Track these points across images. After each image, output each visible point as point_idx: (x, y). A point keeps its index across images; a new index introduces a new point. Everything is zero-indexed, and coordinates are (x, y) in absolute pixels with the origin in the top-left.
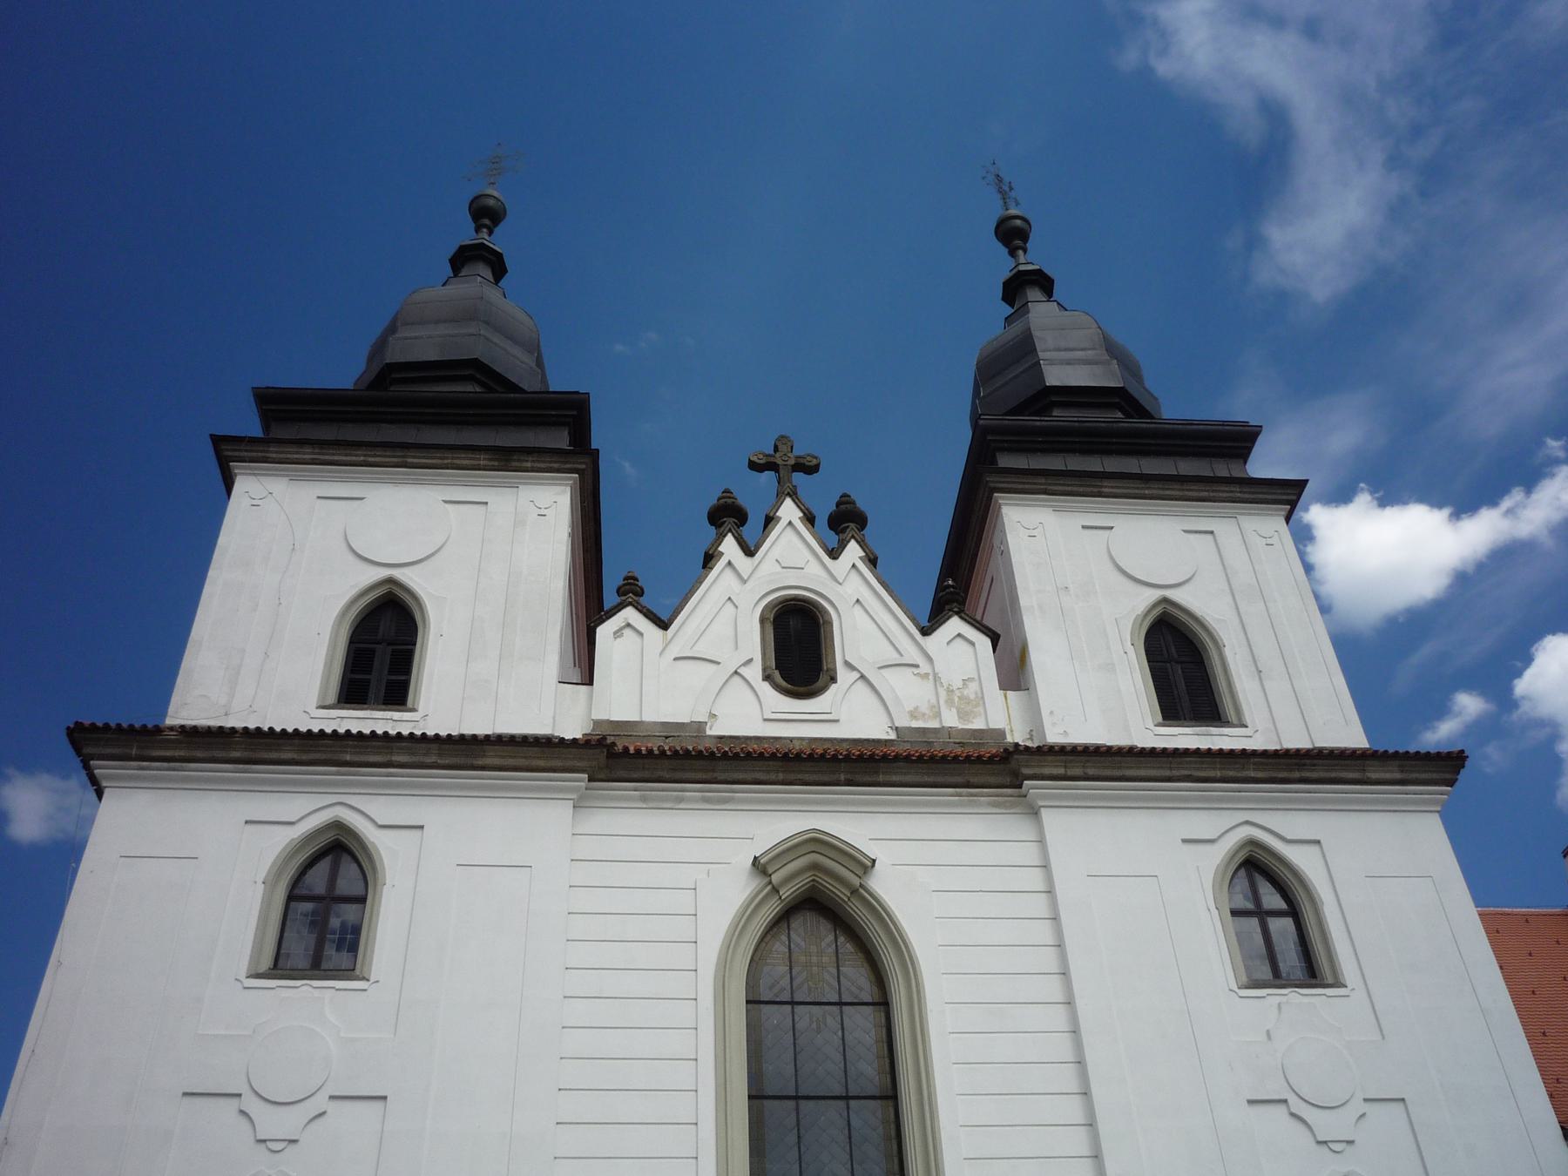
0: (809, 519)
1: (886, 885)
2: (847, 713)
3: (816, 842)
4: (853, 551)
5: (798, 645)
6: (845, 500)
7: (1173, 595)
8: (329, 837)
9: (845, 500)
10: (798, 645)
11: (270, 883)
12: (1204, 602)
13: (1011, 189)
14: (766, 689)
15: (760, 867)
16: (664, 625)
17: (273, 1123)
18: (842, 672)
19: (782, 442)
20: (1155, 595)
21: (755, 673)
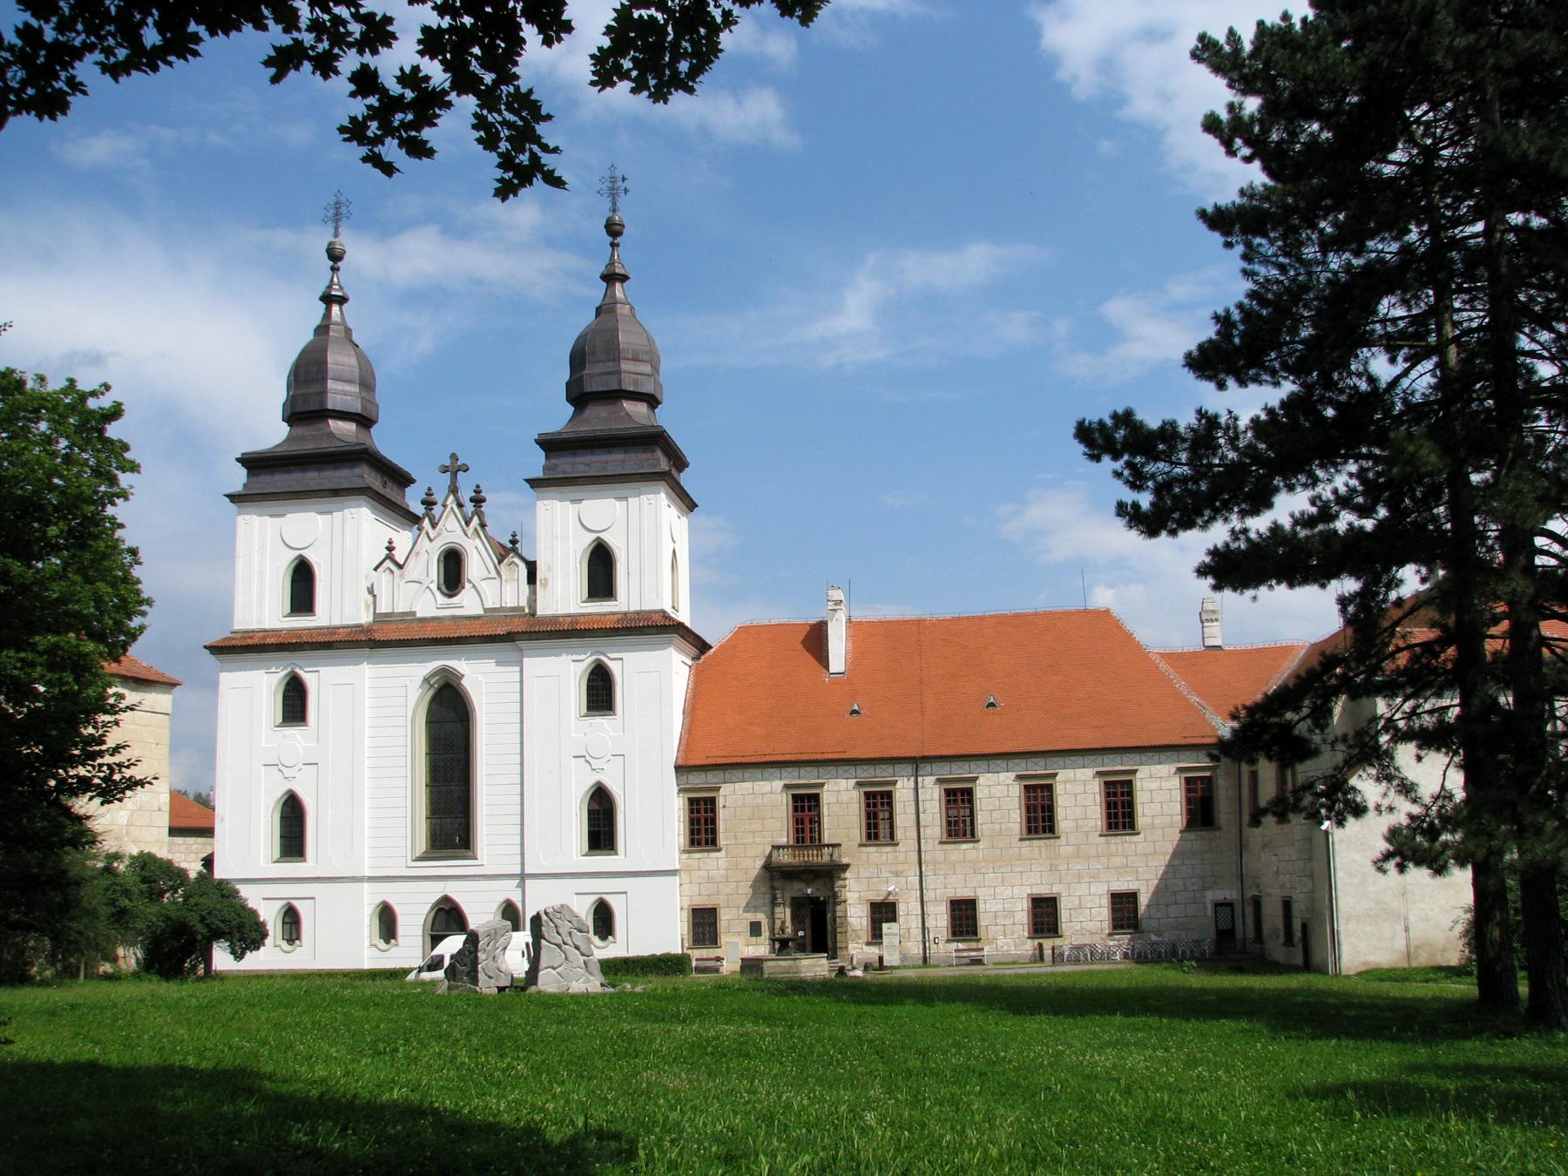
0: (460, 505)
1: (467, 684)
2: (468, 603)
3: (444, 671)
5: (452, 570)
6: (478, 491)
7: (601, 535)
9: (478, 491)
10: (452, 570)
12: (614, 541)
13: (624, 179)
14: (438, 593)
15: (426, 680)
16: (401, 567)
17: (288, 772)
19: (454, 457)
20: (595, 536)
21: (434, 587)
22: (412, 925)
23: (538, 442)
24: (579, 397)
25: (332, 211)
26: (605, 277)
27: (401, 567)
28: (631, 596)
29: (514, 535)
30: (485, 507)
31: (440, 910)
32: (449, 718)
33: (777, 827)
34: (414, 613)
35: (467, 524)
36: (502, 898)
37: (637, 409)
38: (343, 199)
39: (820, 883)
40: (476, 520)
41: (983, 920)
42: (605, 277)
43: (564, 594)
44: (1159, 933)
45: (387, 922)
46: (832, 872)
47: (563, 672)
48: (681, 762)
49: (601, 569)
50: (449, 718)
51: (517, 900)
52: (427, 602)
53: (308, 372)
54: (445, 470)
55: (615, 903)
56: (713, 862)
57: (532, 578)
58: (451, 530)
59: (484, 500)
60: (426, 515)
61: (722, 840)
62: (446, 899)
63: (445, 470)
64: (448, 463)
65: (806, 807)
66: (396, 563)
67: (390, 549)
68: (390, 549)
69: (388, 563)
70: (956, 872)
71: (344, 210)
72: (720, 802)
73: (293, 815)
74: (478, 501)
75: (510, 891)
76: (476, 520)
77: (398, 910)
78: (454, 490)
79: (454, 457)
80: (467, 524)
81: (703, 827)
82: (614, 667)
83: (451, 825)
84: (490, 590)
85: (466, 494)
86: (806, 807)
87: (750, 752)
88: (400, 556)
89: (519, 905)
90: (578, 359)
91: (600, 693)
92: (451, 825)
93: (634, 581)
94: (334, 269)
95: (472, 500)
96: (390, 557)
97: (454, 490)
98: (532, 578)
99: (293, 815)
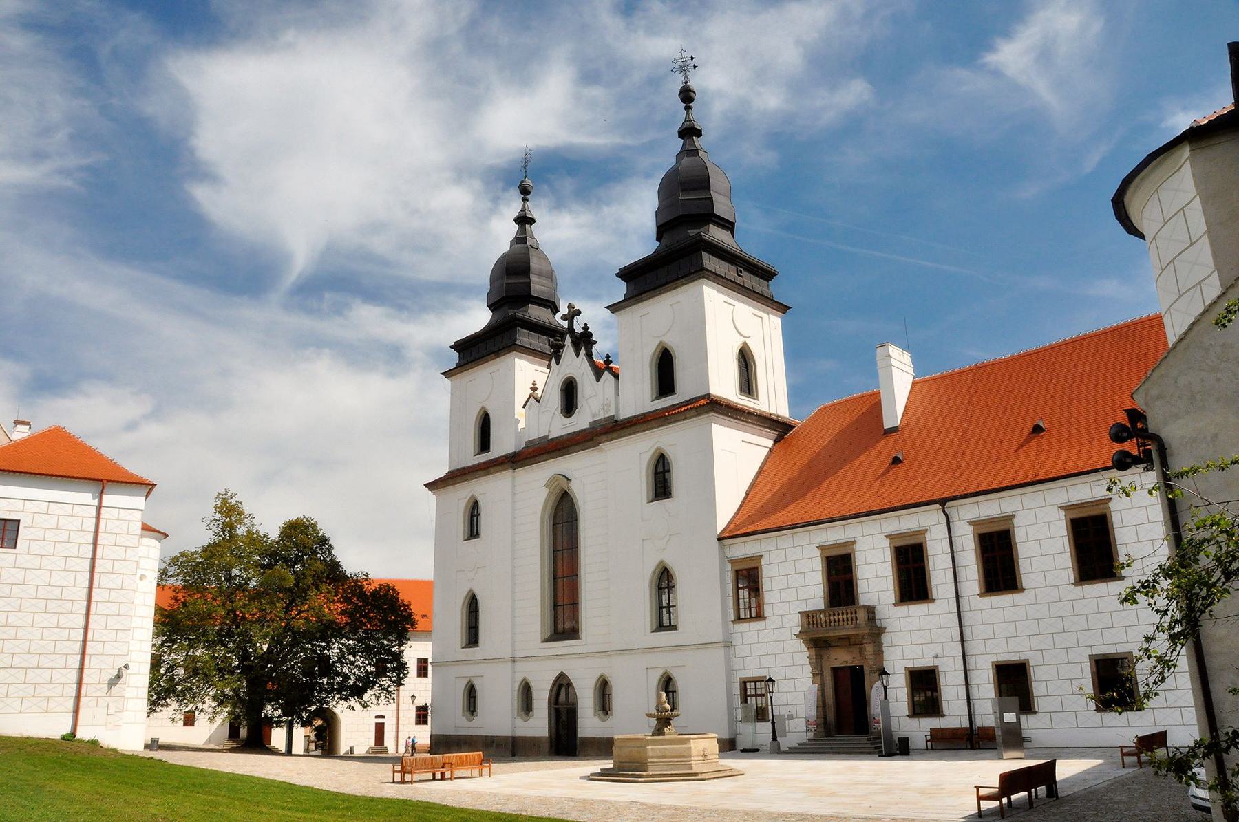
2: (581, 421)
4: (583, 351)
15: (547, 486)
23: (617, 275)
28: (685, 389)
29: (608, 356)
32: (563, 515)
39: (856, 650)
40: (583, 351)
41: (1038, 689)
43: (637, 394)
50: (563, 515)
52: (560, 427)
55: (676, 675)
65: (840, 570)
67: (534, 389)
68: (534, 389)
70: (1002, 627)
73: (473, 607)
86: (840, 570)
99: (473, 607)
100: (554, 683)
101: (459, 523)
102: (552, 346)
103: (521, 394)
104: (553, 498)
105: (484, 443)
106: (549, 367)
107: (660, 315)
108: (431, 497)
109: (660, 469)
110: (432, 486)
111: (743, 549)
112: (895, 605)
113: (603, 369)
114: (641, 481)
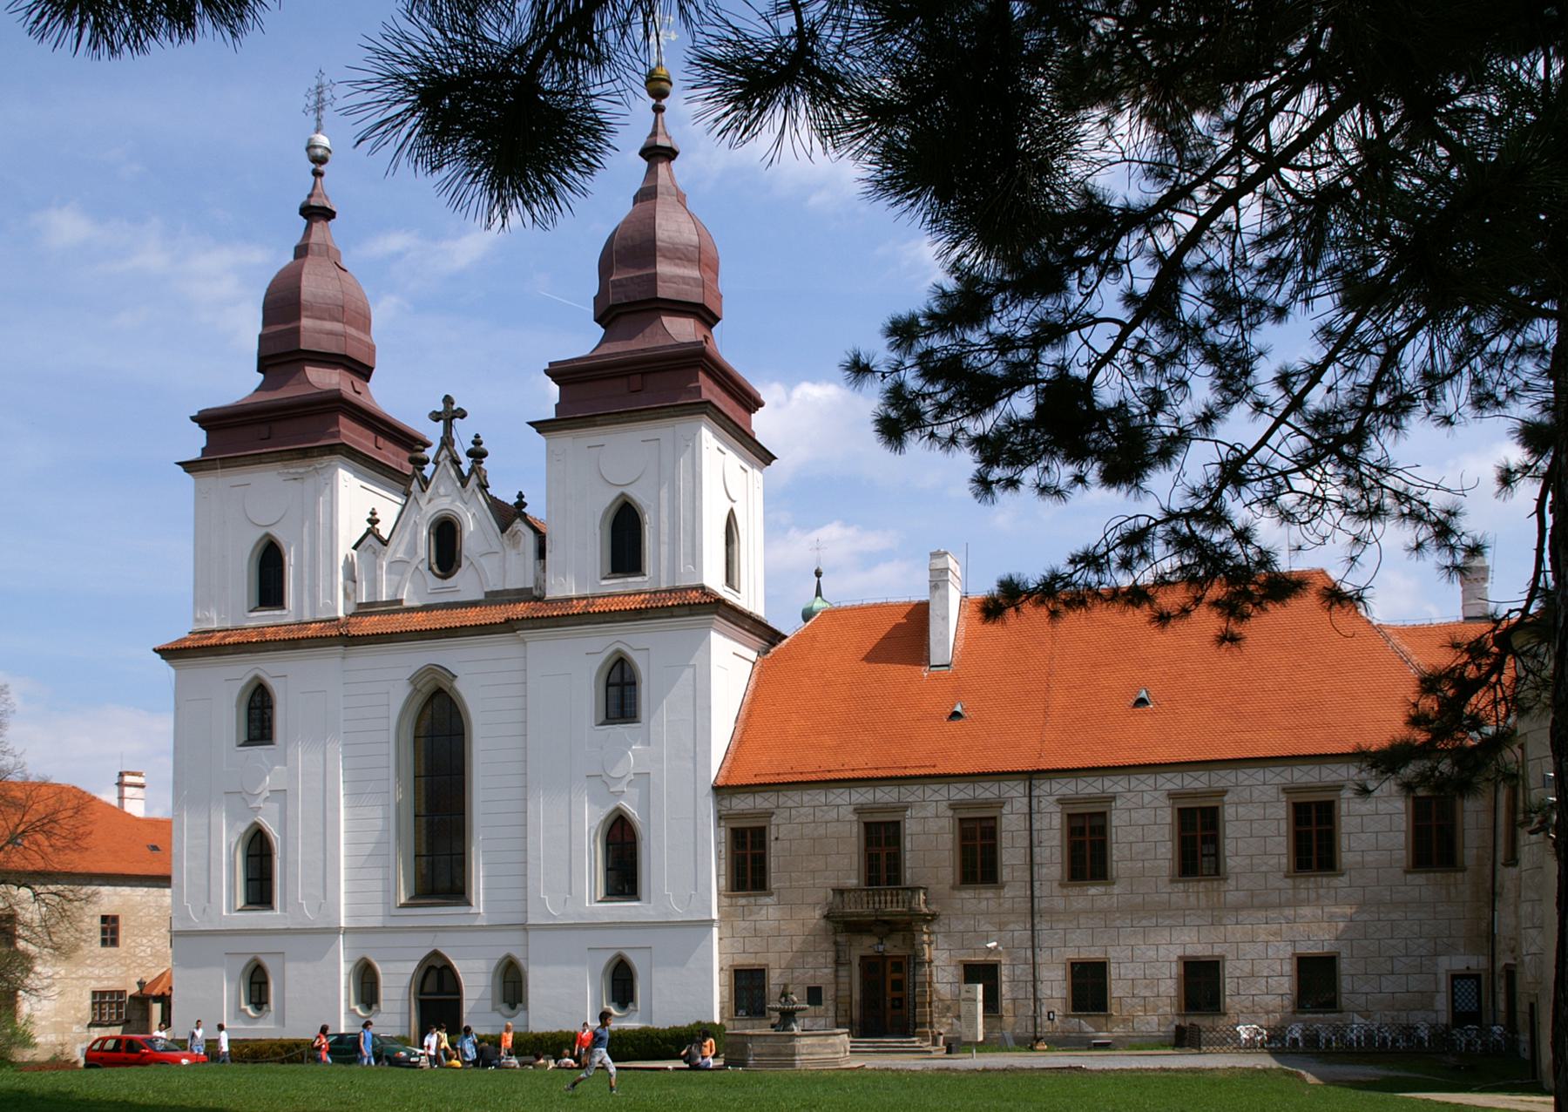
2: (465, 585)
3: (432, 670)
6: (477, 442)
8: (255, 684)
9: (477, 442)
11: (238, 706)
15: (413, 680)
18: (464, 563)
19: (448, 400)
20: (617, 492)
21: (424, 567)
22: (396, 981)
24: (609, 314)
25: (314, 98)
26: (643, 153)
27: (385, 543)
28: (658, 572)
30: (486, 463)
31: (430, 969)
33: (845, 865)
34: (401, 601)
35: (464, 485)
36: (502, 955)
37: (682, 330)
38: (325, 80)
39: (898, 938)
40: (473, 481)
42: (643, 153)
44: (1366, 1013)
45: (367, 984)
46: (907, 926)
47: (575, 663)
48: (721, 782)
49: (625, 538)
51: (518, 954)
53: (282, 304)
54: (436, 416)
56: (767, 912)
57: (541, 553)
58: (443, 498)
59: (485, 454)
60: (415, 475)
61: (774, 881)
62: (436, 954)
63: (436, 416)
64: (440, 408)
66: (379, 539)
67: (373, 521)
68: (373, 521)
69: (370, 539)
71: (327, 95)
72: (772, 833)
74: (477, 454)
75: (508, 945)
76: (473, 481)
77: (379, 967)
78: (447, 442)
79: (448, 400)
80: (464, 485)
81: (748, 864)
82: (638, 659)
83: (439, 867)
84: (491, 563)
85: (462, 446)
87: (814, 764)
88: (384, 530)
89: (522, 962)
90: (607, 263)
91: (621, 696)
92: (439, 867)
93: (664, 549)
94: (317, 174)
95: (470, 454)
96: (372, 532)
97: (447, 442)
98: (541, 553)
100: (420, 966)
101: (228, 717)
102: (412, 461)
103: (350, 527)
104: (420, 699)
105: (270, 590)
106: (407, 494)
107: (621, 456)
108: (165, 671)
109: (616, 677)
110: (167, 653)
111: (742, 803)
112: (953, 888)
113: (508, 515)
114: (586, 693)
